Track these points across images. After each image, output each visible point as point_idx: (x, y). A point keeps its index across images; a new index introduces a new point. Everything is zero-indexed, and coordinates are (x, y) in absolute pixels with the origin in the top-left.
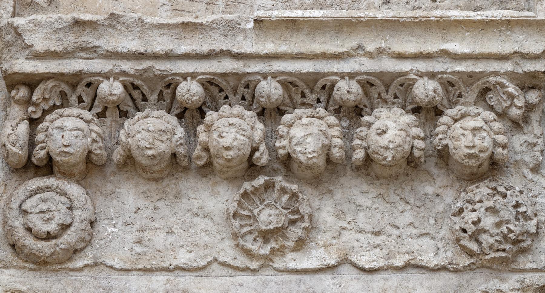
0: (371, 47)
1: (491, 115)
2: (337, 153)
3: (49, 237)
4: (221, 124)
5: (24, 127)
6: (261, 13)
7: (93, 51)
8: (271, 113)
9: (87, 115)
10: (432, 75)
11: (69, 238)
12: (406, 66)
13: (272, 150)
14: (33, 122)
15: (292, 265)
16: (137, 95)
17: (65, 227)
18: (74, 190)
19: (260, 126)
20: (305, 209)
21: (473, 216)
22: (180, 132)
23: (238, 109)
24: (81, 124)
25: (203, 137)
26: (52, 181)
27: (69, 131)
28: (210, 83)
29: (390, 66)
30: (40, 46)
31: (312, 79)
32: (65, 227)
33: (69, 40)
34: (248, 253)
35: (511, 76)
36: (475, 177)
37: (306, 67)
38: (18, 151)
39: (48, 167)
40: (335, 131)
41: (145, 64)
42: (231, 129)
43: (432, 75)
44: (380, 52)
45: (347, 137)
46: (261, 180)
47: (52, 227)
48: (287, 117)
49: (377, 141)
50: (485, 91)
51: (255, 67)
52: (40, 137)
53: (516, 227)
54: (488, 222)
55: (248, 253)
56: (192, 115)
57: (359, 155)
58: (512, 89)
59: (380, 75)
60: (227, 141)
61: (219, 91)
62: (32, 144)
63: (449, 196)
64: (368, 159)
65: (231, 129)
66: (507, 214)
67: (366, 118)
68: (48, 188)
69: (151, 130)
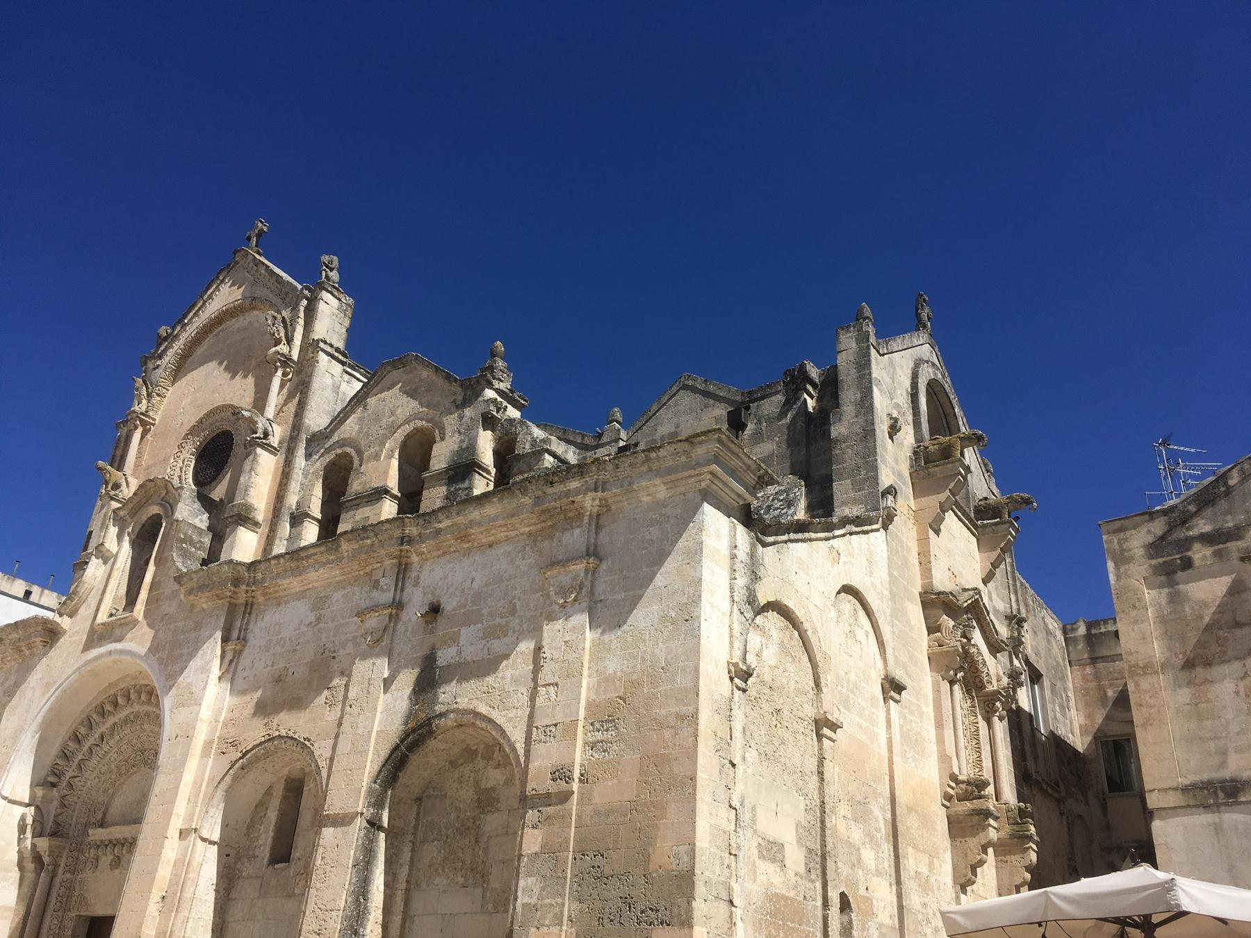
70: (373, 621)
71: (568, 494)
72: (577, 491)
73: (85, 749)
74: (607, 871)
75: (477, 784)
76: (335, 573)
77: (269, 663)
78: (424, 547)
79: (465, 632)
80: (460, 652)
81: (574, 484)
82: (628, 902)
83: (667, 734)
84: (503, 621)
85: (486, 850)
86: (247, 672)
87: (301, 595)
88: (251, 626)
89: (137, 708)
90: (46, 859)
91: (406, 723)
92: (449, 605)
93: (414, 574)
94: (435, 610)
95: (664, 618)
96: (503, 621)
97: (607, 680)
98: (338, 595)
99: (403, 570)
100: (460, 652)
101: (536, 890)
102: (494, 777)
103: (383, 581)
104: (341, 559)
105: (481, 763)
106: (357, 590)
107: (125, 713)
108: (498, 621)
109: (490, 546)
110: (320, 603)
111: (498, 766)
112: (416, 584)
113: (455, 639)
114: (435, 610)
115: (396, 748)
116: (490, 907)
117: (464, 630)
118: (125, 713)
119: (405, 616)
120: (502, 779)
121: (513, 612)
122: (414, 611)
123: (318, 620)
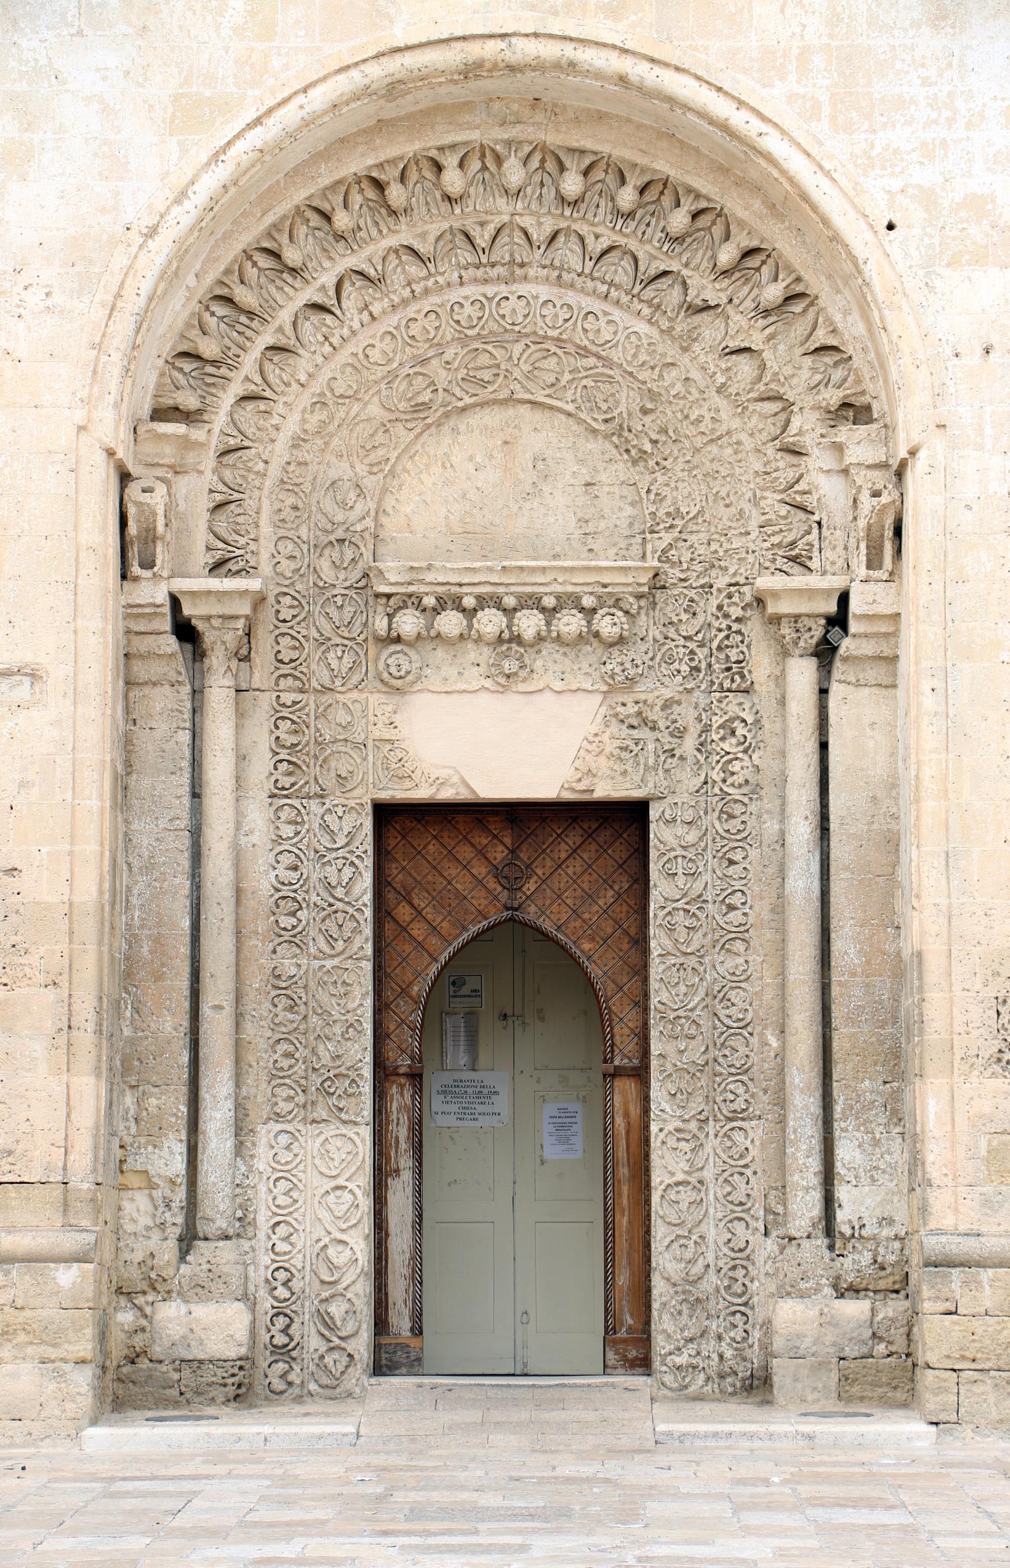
0: (560, 580)
1: (620, 614)
2: (543, 634)
3: (401, 677)
4: (485, 621)
5: (386, 619)
6: (505, 563)
7: (421, 581)
8: (510, 613)
9: (417, 613)
10: (591, 593)
11: (410, 678)
12: (578, 589)
13: (511, 632)
14: (390, 616)
15: (521, 689)
16: (441, 605)
17: (408, 673)
18: (412, 653)
19: (505, 620)
20: (527, 661)
21: (611, 667)
22: (465, 623)
23: (494, 611)
24: (415, 620)
25: (476, 625)
26: (399, 647)
27: (408, 623)
28: (479, 598)
29: (570, 589)
30: (392, 580)
31: (531, 596)
32: (408, 673)
33: (407, 578)
34: (499, 684)
35: (631, 594)
36: (612, 645)
37: (529, 589)
38: (383, 633)
39: (398, 640)
40: (543, 622)
41: (448, 587)
42: (490, 622)
43: (591, 593)
44: (565, 582)
45: (548, 624)
46: (504, 648)
47: (402, 673)
48: (518, 614)
49: (565, 630)
50: (618, 600)
51: (501, 590)
52: (394, 626)
53: (632, 672)
54: (618, 670)
55: (499, 684)
56: (470, 614)
57: (554, 634)
58: (631, 600)
59: (565, 593)
60: (489, 629)
61: (483, 602)
62: (390, 629)
63: (600, 651)
64: (558, 635)
65: (490, 622)
66: (628, 665)
67: (558, 615)
68: (398, 652)
69: (450, 622)
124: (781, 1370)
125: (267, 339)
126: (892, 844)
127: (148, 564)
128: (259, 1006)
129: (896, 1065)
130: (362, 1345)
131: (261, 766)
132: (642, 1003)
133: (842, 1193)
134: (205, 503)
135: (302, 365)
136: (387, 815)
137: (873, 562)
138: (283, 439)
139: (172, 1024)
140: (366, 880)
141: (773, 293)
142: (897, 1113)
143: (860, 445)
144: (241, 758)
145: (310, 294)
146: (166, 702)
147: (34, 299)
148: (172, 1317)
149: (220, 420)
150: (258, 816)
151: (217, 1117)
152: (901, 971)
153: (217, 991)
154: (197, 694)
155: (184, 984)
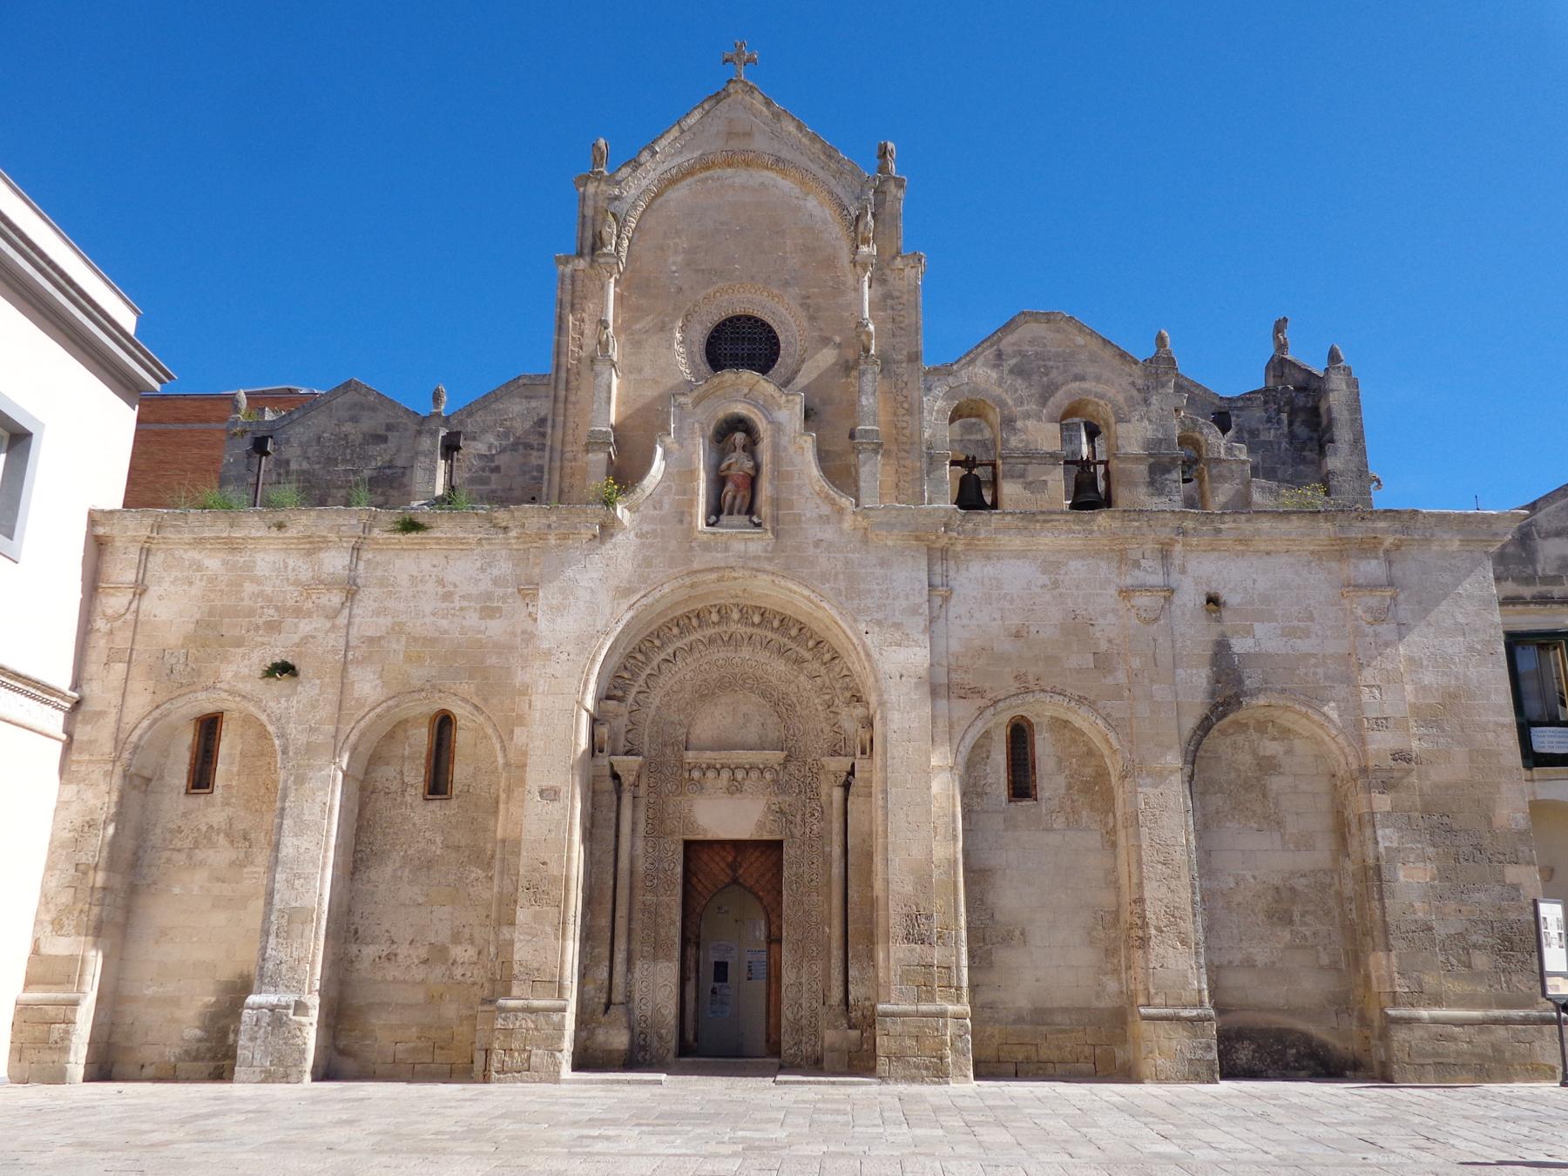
70: (1143, 600)
71: (1374, 530)
72: (1386, 531)
73: (655, 663)
74: (1455, 827)
75: (1254, 753)
76: (1077, 542)
77: (997, 615)
78: (1194, 541)
79: (1257, 625)
80: (1257, 643)
81: (1382, 524)
82: (1479, 848)
83: (1490, 736)
84: (1302, 624)
85: (1276, 805)
86: (965, 621)
87: (1021, 555)
88: (952, 573)
89: (733, 627)
90: (628, 779)
91: (1213, 694)
92: (1231, 598)
93: (1177, 562)
94: (1213, 600)
95: (1471, 649)
96: (1302, 624)
97: (1424, 688)
98: (1074, 564)
99: (1165, 554)
100: (1257, 643)
101: (1395, 837)
102: (1271, 748)
103: (1143, 562)
104: (1092, 532)
105: (1255, 736)
106: (1103, 564)
107: (710, 631)
108: (1295, 623)
109: (1268, 553)
110: (1051, 566)
111: (1274, 739)
112: (1183, 571)
113: (1249, 632)
114: (1213, 600)
115: (1207, 718)
116: (1291, 846)
117: (1257, 625)
118: (710, 631)
119: (1177, 599)
120: (1281, 750)
121: (1311, 618)
122: (1190, 597)
123: (1056, 585)
124: (827, 1056)
125: (648, 671)
126: (870, 856)
127: (601, 751)
128: (638, 915)
129: (870, 939)
130: (673, 1043)
131: (641, 827)
132: (780, 916)
133: (850, 987)
134: (624, 730)
135: (661, 681)
136: (689, 845)
137: (863, 753)
138: (653, 707)
139: (604, 921)
140: (679, 869)
141: (827, 657)
142: (871, 957)
143: (859, 711)
144: (634, 824)
145: (663, 656)
146: (608, 799)
147: (564, 657)
148: (600, 1036)
149: (630, 699)
150: (640, 844)
151: (620, 957)
152: (872, 903)
153: (622, 911)
154: (619, 799)
155: (610, 906)
